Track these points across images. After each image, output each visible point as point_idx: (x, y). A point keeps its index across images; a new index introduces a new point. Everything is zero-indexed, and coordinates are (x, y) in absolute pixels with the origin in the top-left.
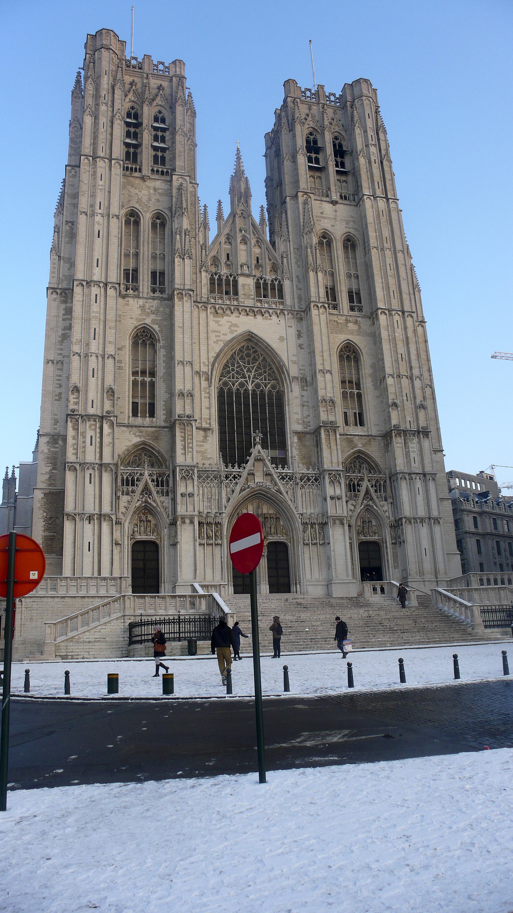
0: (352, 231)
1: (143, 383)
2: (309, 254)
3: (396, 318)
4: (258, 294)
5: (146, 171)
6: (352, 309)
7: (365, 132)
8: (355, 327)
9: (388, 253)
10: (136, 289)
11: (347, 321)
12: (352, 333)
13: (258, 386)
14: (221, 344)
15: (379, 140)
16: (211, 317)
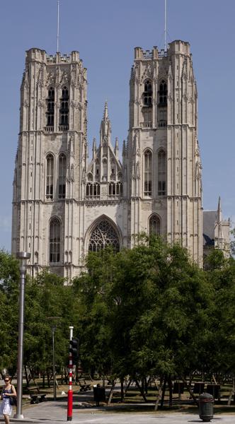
0: (163, 146)
1: (55, 244)
2: (133, 169)
3: (176, 201)
4: (110, 193)
5: (56, 130)
6: (160, 194)
7: (174, 80)
8: (160, 205)
9: (177, 161)
10: (51, 197)
11: (155, 202)
12: (157, 209)
13: (108, 242)
14: (90, 223)
15: (182, 83)
16: (85, 207)
